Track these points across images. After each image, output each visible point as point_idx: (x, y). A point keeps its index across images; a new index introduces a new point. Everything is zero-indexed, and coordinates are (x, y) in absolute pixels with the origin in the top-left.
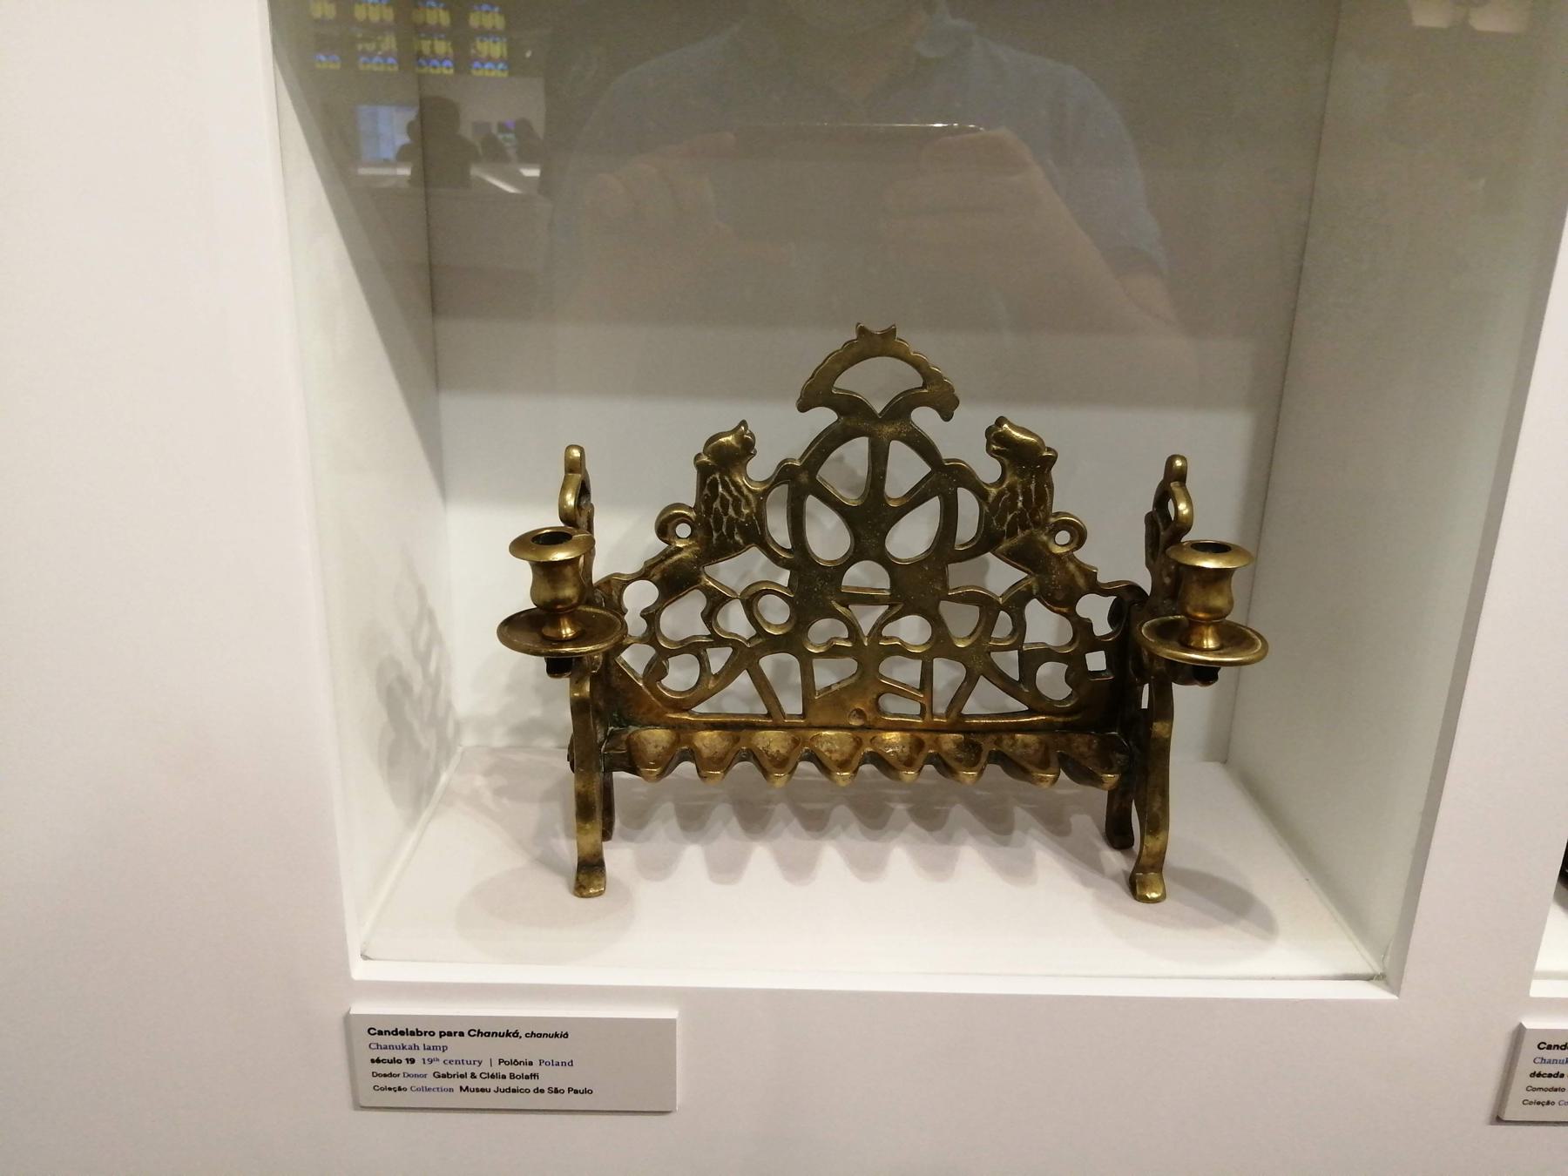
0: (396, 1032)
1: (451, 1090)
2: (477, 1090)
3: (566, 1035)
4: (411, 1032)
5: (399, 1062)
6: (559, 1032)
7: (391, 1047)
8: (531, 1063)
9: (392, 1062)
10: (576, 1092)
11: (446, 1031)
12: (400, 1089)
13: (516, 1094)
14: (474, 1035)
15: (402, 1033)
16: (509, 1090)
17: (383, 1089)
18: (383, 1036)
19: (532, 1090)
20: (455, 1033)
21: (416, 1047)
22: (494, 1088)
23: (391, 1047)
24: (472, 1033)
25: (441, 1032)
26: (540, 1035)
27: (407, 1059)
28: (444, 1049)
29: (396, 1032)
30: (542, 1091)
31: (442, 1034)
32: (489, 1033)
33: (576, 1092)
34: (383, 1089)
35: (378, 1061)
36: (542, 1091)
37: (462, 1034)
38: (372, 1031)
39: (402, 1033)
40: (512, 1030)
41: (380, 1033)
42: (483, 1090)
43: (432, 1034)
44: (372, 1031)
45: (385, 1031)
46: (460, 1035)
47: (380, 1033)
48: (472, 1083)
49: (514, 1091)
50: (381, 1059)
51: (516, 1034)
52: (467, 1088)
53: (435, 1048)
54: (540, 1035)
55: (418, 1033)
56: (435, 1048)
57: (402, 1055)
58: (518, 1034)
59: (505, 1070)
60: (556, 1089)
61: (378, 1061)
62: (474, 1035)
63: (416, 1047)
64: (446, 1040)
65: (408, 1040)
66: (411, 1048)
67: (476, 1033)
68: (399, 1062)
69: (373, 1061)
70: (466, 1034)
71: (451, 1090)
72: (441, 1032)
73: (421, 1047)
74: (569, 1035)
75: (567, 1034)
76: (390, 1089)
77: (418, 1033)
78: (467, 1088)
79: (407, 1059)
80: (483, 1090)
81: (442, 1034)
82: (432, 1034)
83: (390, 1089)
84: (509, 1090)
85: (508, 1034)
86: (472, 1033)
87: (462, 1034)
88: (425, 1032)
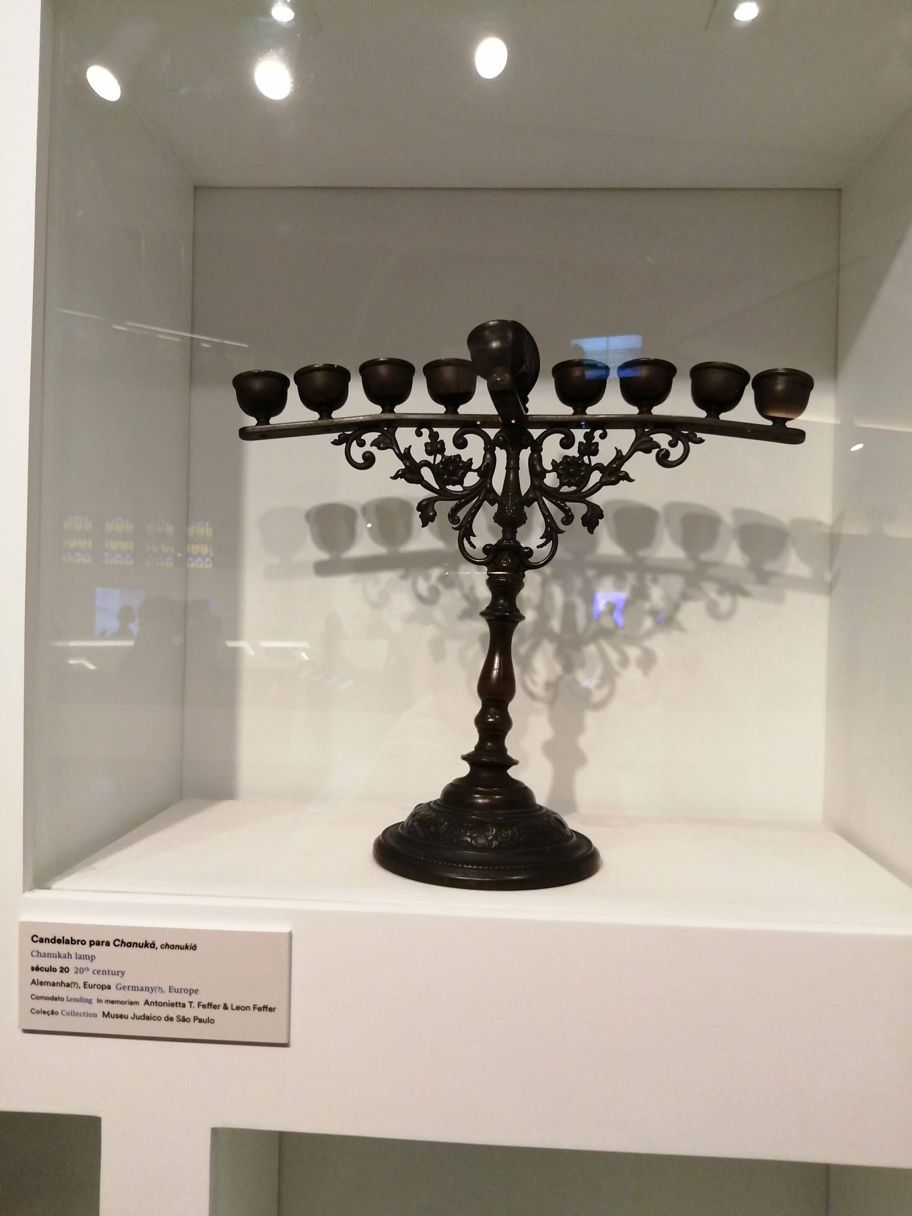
0: (55, 941)
1: (95, 1015)
3: (194, 948)
7: (49, 955)
19: (163, 1018)
20: (103, 942)
23: (49, 955)
24: (117, 943)
25: (91, 941)
26: (173, 947)
29: (55, 941)
31: (92, 943)
32: (131, 943)
37: (108, 944)
38: (35, 939)
39: (59, 941)
40: (150, 941)
42: (121, 1016)
43: (83, 942)
44: (35, 939)
46: (106, 945)
47: (41, 940)
49: (148, 1018)
51: (153, 945)
52: (109, 1013)
54: (173, 947)
55: (72, 942)
58: (154, 945)
62: (119, 945)
65: (63, 948)
67: (120, 943)
70: (111, 944)
71: (95, 1015)
75: (195, 946)
77: (72, 942)
78: (109, 1013)
80: (121, 1016)
81: (92, 943)
82: (83, 942)
85: (146, 945)
86: (117, 943)
87: (108, 944)
88: (78, 941)
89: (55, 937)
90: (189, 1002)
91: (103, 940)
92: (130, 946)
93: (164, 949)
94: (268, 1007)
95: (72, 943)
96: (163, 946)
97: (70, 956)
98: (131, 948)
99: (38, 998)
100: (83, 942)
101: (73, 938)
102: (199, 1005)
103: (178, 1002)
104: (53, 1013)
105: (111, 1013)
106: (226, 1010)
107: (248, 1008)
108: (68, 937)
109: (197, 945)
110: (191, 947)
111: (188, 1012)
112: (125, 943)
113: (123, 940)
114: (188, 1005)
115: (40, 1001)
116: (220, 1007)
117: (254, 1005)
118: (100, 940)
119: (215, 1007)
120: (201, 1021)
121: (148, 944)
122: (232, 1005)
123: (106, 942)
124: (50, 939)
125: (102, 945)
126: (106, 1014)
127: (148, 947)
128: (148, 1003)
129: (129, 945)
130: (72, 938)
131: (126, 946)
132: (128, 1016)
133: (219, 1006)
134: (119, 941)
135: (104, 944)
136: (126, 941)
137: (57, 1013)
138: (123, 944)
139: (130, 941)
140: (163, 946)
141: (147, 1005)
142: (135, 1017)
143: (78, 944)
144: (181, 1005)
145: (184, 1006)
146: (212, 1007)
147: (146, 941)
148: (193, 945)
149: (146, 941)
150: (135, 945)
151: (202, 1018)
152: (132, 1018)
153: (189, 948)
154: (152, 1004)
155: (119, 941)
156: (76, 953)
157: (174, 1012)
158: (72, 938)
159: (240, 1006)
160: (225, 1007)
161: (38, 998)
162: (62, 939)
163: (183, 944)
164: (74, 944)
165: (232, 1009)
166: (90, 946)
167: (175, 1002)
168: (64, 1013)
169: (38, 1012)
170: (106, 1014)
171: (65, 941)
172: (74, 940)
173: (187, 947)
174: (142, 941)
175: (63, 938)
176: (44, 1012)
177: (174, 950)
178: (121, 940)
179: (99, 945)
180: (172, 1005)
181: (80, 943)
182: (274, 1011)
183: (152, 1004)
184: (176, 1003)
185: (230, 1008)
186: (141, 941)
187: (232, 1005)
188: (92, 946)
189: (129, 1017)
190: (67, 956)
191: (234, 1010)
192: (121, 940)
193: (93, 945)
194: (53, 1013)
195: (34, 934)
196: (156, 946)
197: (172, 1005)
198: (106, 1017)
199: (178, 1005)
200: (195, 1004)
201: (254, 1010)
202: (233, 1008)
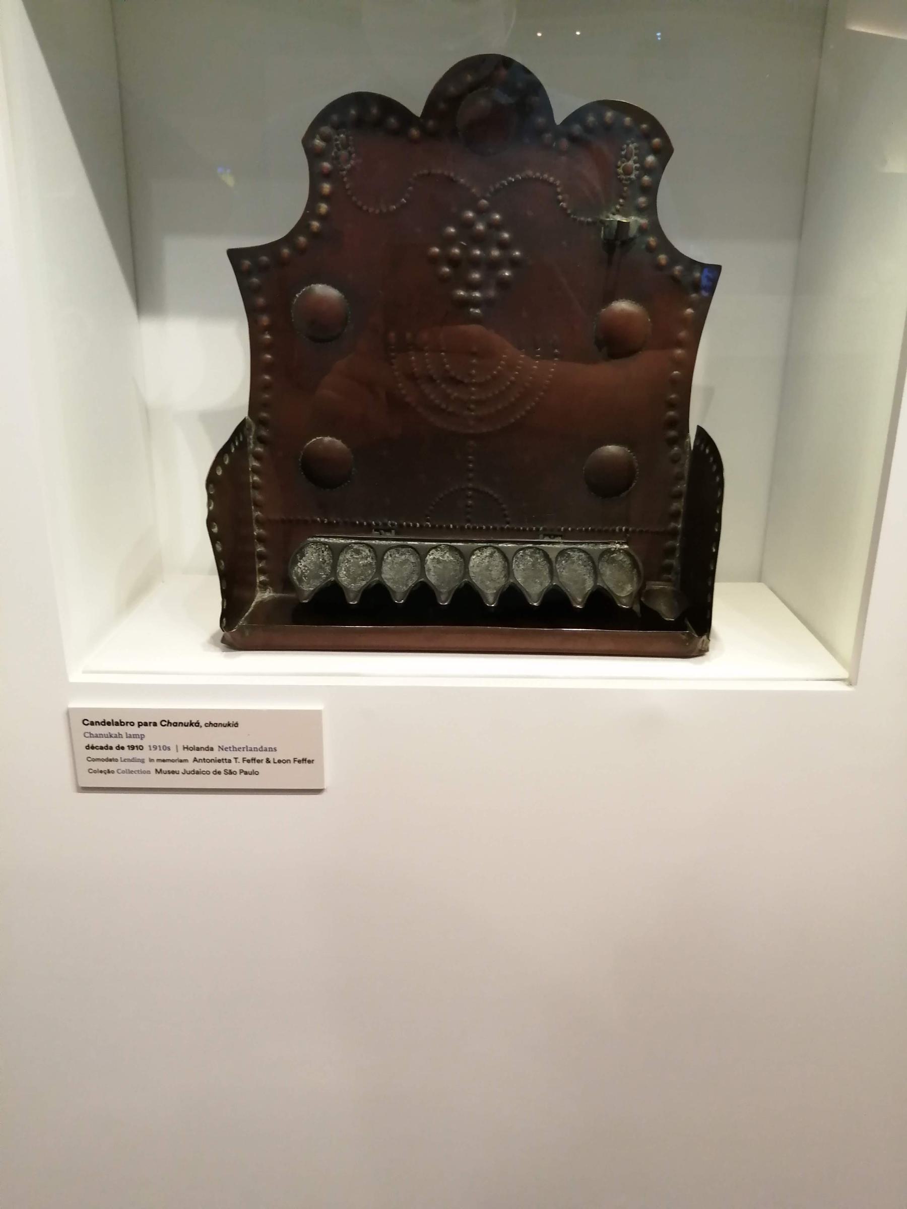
1: (149, 772)
2: (169, 772)
3: (236, 725)
4: (116, 722)
6: (231, 722)
8: (212, 749)
11: (143, 722)
13: (199, 775)
15: (109, 724)
19: (211, 772)
20: (150, 723)
21: (119, 736)
22: (182, 771)
24: (164, 723)
26: (216, 725)
28: (142, 737)
30: (219, 773)
36: (219, 773)
37: (155, 724)
39: (109, 724)
40: (194, 721)
42: (173, 772)
43: (132, 724)
46: (154, 725)
48: (166, 767)
49: (198, 773)
51: (197, 724)
52: (161, 770)
53: (135, 736)
54: (216, 725)
56: (135, 736)
57: (113, 742)
58: (199, 723)
59: (190, 755)
63: (119, 736)
66: (116, 737)
67: (166, 723)
71: (149, 772)
72: (139, 723)
73: (124, 736)
80: (173, 772)
82: (132, 724)
85: (191, 724)
86: (164, 723)
87: (155, 724)
88: (127, 723)
91: (150, 721)
92: (176, 726)
93: (208, 727)
94: (307, 759)
95: (121, 725)
96: (207, 725)
99: (94, 760)
101: (122, 721)
102: (244, 760)
103: (224, 758)
104: (109, 772)
109: (238, 723)
110: (233, 724)
111: (233, 766)
112: (171, 723)
113: (168, 721)
114: (233, 761)
115: (95, 762)
118: (148, 722)
120: (246, 773)
121: (193, 723)
123: (154, 722)
124: (100, 721)
125: (150, 726)
126: (159, 770)
127: (193, 726)
130: (120, 720)
131: (172, 725)
132: (179, 771)
135: (152, 724)
136: (172, 721)
137: (113, 772)
138: (170, 724)
139: (176, 722)
140: (206, 725)
141: (196, 762)
142: (185, 772)
143: (127, 725)
145: (230, 761)
146: (256, 761)
147: (191, 721)
149: (191, 721)
151: (247, 771)
153: (231, 725)
156: (126, 733)
157: (221, 767)
158: (120, 720)
161: (94, 760)
162: (111, 721)
164: (123, 725)
166: (139, 727)
167: (221, 759)
168: (120, 771)
169: (95, 772)
170: (159, 770)
171: (114, 723)
172: (123, 722)
173: (229, 725)
175: (113, 720)
176: (101, 772)
179: (147, 726)
180: (219, 761)
181: (128, 724)
182: (313, 763)
188: (141, 727)
189: (180, 773)
193: (141, 726)
194: (109, 772)
195: (83, 725)
197: (219, 761)
198: (159, 773)
200: (240, 760)
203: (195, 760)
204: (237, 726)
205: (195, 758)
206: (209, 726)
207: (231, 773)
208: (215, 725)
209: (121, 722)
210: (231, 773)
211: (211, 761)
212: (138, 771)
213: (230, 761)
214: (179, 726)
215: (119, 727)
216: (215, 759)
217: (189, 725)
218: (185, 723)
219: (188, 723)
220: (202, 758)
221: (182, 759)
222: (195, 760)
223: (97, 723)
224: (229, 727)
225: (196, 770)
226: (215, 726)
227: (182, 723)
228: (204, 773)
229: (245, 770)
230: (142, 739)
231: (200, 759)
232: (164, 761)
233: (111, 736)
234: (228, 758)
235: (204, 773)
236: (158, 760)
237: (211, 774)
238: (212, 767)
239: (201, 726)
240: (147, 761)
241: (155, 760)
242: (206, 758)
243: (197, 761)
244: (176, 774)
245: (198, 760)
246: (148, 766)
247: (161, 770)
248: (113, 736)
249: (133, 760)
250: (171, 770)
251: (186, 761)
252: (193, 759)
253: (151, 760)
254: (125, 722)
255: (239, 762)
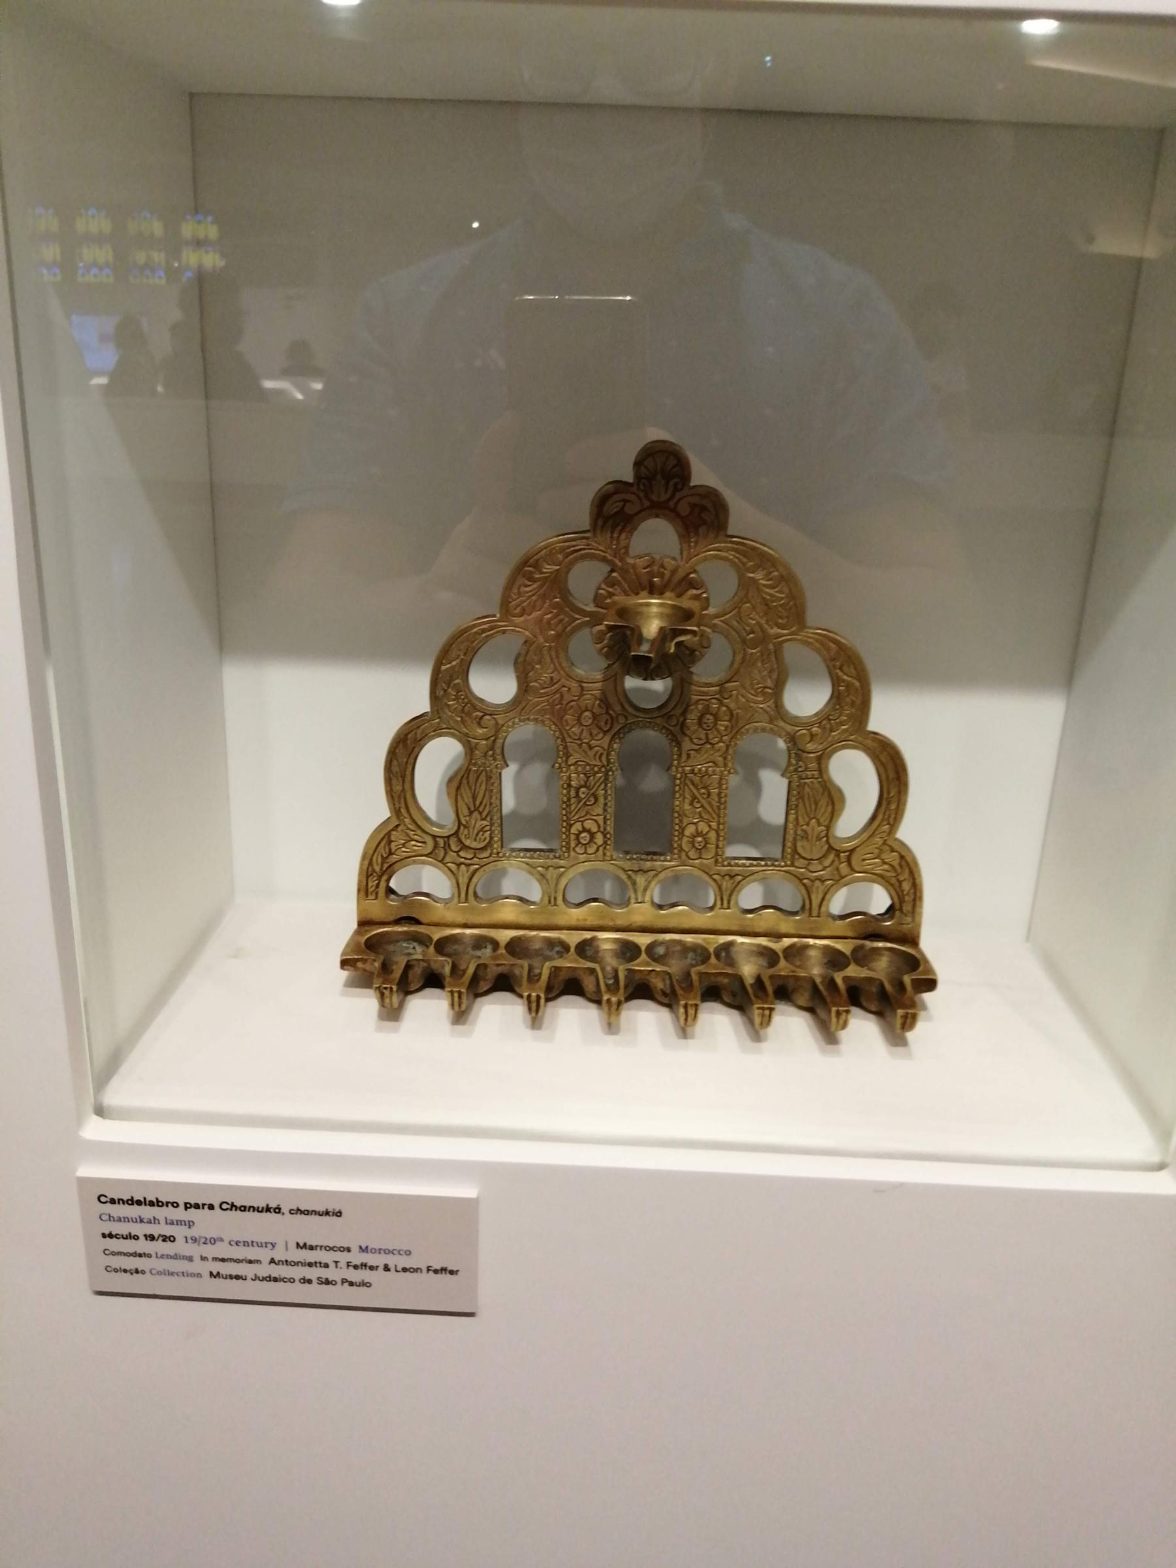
0: (131, 1202)
1: (199, 1275)
2: (231, 1277)
3: (339, 1214)
4: (150, 1201)
5: (136, 1238)
7: (127, 1220)
9: (126, 1238)
10: (351, 1284)
12: (137, 1272)
14: (227, 1209)
15: (139, 1203)
16: (270, 1279)
17: (116, 1271)
18: (116, 1206)
19: (297, 1280)
20: (204, 1205)
21: (154, 1221)
22: (251, 1275)
23: (127, 1220)
24: (225, 1206)
25: (186, 1204)
26: (307, 1213)
27: (145, 1236)
28: (190, 1224)
29: (131, 1202)
30: (310, 1281)
31: (187, 1206)
32: (245, 1207)
33: (351, 1284)
34: (116, 1271)
35: (111, 1236)
36: (310, 1281)
37: (211, 1207)
38: (103, 1199)
39: (139, 1203)
40: (273, 1205)
41: (113, 1201)
42: (237, 1277)
43: (175, 1205)
44: (103, 1199)
45: (119, 1200)
47: (113, 1201)
49: (276, 1280)
50: (114, 1233)
51: (278, 1210)
52: (218, 1273)
53: (179, 1223)
54: (307, 1213)
55: (158, 1203)
56: (179, 1223)
57: (139, 1229)
58: (280, 1209)
59: (264, 1255)
60: (327, 1279)
61: (111, 1236)
62: (227, 1209)
63: (154, 1221)
64: (193, 1214)
65: (146, 1212)
67: (229, 1207)
68: (136, 1238)
69: (104, 1236)
71: (199, 1275)
72: (186, 1204)
73: (163, 1221)
74: (343, 1214)
75: (340, 1212)
76: (125, 1271)
77: (158, 1203)
79: (145, 1236)
80: (237, 1277)
81: (187, 1206)
82: (175, 1205)
83: (125, 1271)
84: (270, 1279)
85: (268, 1209)
86: (225, 1206)
87: (211, 1207)
89: (132, 1197)
90: (334, 1261)
91: (204, 1202)
92: (244, 1211)
93: (294, 1215)
95: (158, 1206)
96: (292, 1212)
97: (156, 1221)
98: (247, 1213)
100: (175, 1205)
101: (160, 1199)
102: (348, 1266)
103: (318, 1261)
105: (221, 1273)
106: (388, 1273)
107: (419, 1271)
108: (151, 1197)
109: (343, 1211)
110: (333, 1213)
112: (236, 1206)
113: (233, 1203)
114: (332, 1265)
116: (379, 1268)
117: (428, 1267)
119: (372, 1268)
121: (271, 1208)
122: (396, 1266)
123: (209, 1205)
124: (125, 1199)
125: (203, 1208)
126: (215, 1273)
127: (270, 1212)
128: (274, 1262)
129: (242, 1209)
130: (157, 1199)
132: (246, 1276)
133: (377, 1267)
134: (228, 1204)
135: (206, 1207)
136: (238, 1204)
138: (234, 1208)
140: (291, 1212)
141: (273, 1264)
142: (256, 1278)
144: (322, 1265)
145: (327, 1266)
147: (268, 1205)
148: (337, 1211)
149: (268, 1205)
150: (252, 1209)
152: (252, 1279)
153: (331, 1214)
154: (281, 1263)
155: (228, 1204)
156: (166, 1218)
157: (313, 1273)
158: (157, 1199)
159: (408, 1267)
160: (387, 1268)
162: (143, 1200)
163: (322, 1209)
164: (161, 1206)
165: (397, 1271)
170: (215, 1273)
171: (147, 1203)
172: (161, 1202)
173: (327, 1213)
174: (262, 1204)
175: (145, 1198)
177: (309, 1217)
178: (230, 1203)
180: (310, 1265)
181: (170, 1205)
183: (281, 1263)
184: (316, 1263)
185: (393, 1269)
186: (262, 1204)
187: (396, 1266)
188: (188, 1210)
189: (248, 1278)
190: (153, 1221)
191: (399, 1271)
192: (230, 1203)
196: (282, 1211)
197: (310, 1265)
198: (215, 1277)
199: (318, 1265)
200: (343, 1264)
201: (428, 1272)
202: (398, 1270)
203: (272, 1261)
204: (340, 1216)
205: (273, 1259)
206: (297, 1213)
207: (328, 1282)
208: (306, 1212)
209: (158, 1201)
210: (328, 1282)
211: (296, 1264)
212: (183, 1273)
213: (327, 1266)
214: (249, 1211)
215: (156, 1209)
216: (303, 1261)
217: (265, 1210)
218: (258, 1208)
219: (263, 1208)
220: (283, 1259)
221: (252, 1259)
222: (272, 1261)
223: (121, 1202)
224: (328, 1216)
225: (273, 1276)
226: (305, 1214)
227: (253, 1207)
228: (285, 1280)
229: (349, 1280)
230: (190, 1227)
231: (279, 1261)
232: (223, 1260)
233: (141, 1221)
234: (323, 1261)
235: (285, 1280)
236: (215, 1259)
237: (297, 1282)
238: (298, 1272)
239: (283, 1214)
240: (197, 1259)
241: (210, 1259)
242: (289, 1260)
243: (274, 1262)
244: (241, 1280)
245: (277, 1261)
246: (197, 1266)
247: (218, 1273)
248: (145, 1220)
249: (176, 1257)
250: (234, 1274)
251: (258, 1261)
252: (269, 1259)
253: (203, 1259)
254: (164, 1202)
255: (341, 1268)
